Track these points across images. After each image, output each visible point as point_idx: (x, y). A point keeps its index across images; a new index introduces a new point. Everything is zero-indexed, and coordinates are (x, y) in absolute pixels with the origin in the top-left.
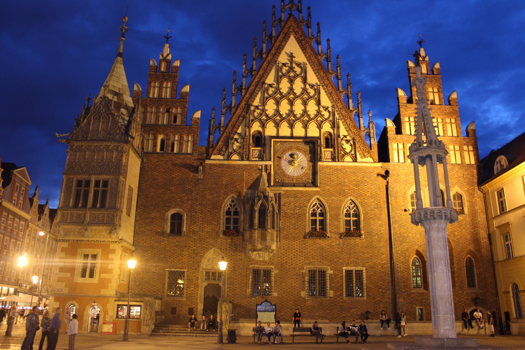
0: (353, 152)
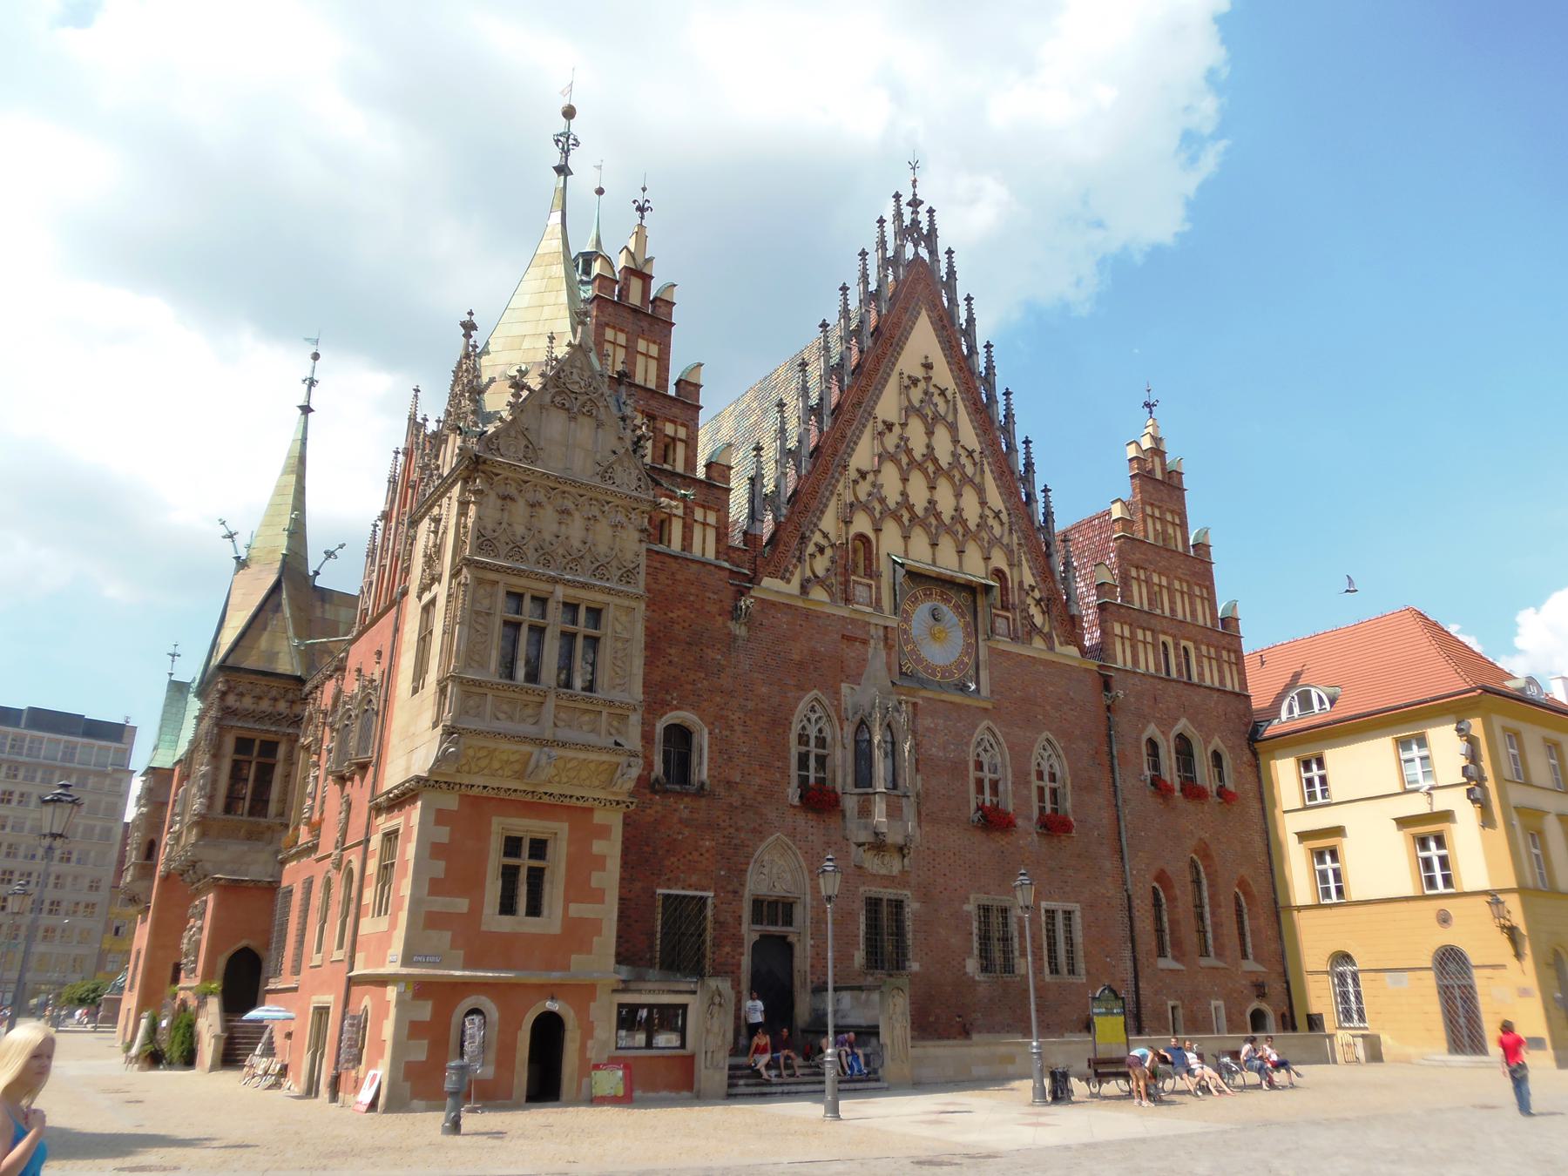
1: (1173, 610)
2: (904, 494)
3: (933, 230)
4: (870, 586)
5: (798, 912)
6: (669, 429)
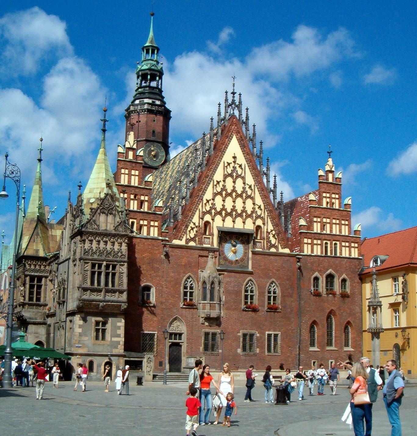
0: (277, 244)
1: (331, 231)
2: (223, 206)
3: (240, 102)
4: (209, 238)
5: (183, 336)
6: (142, 198)
